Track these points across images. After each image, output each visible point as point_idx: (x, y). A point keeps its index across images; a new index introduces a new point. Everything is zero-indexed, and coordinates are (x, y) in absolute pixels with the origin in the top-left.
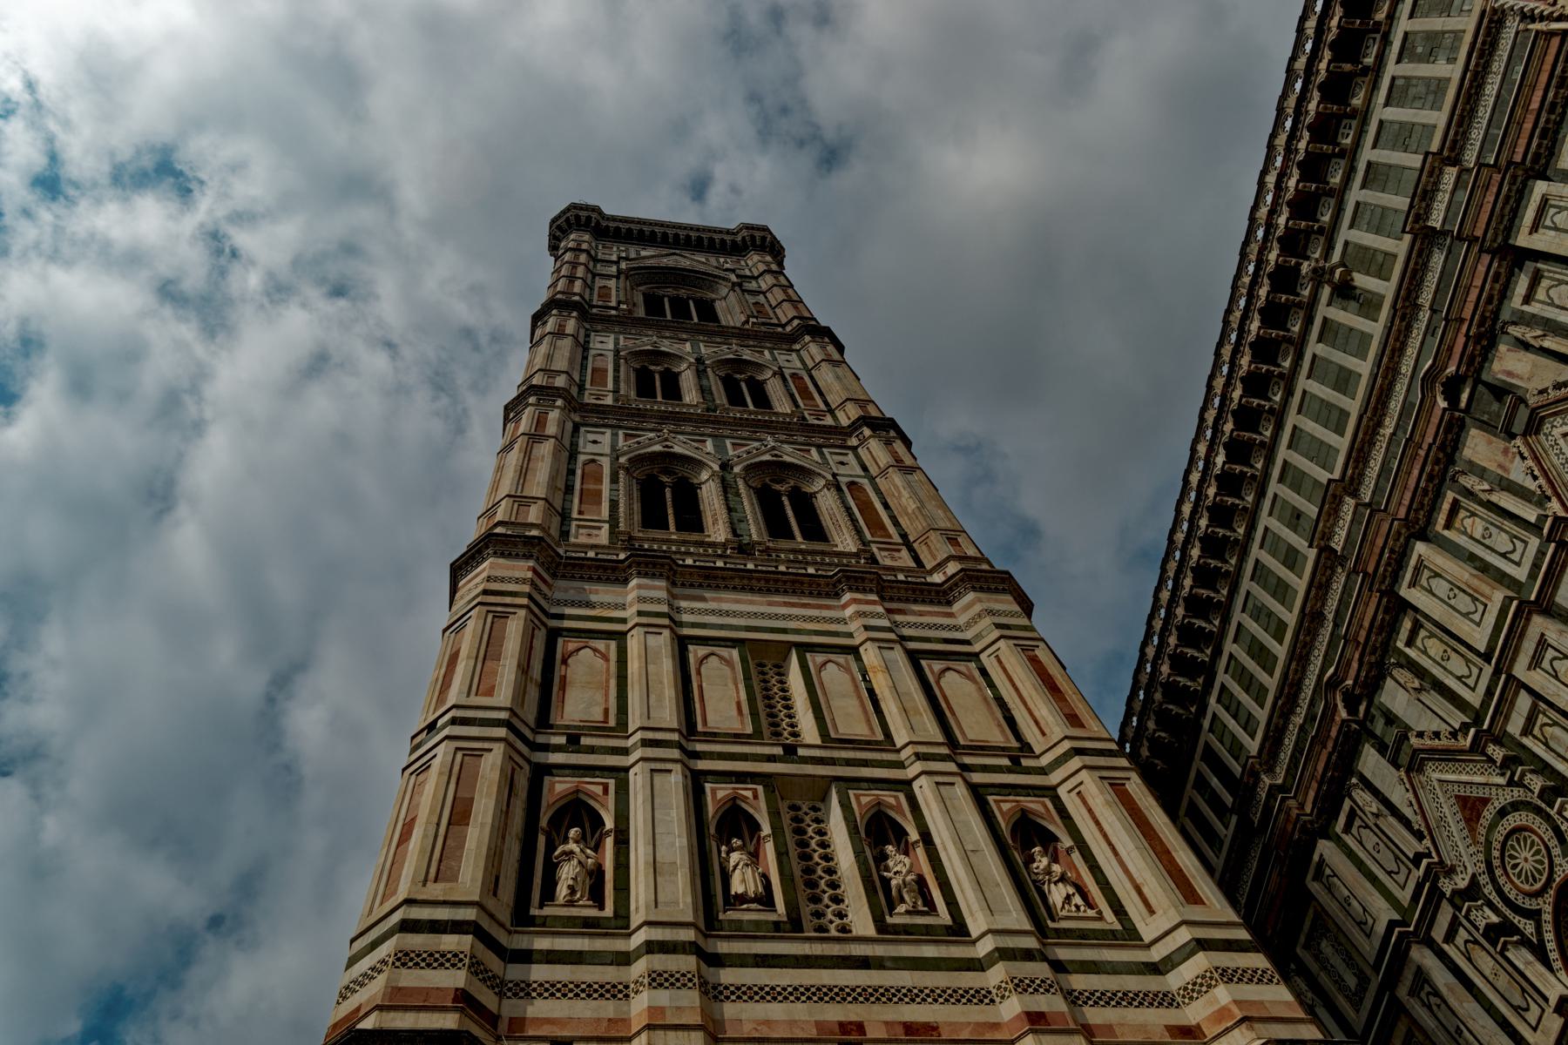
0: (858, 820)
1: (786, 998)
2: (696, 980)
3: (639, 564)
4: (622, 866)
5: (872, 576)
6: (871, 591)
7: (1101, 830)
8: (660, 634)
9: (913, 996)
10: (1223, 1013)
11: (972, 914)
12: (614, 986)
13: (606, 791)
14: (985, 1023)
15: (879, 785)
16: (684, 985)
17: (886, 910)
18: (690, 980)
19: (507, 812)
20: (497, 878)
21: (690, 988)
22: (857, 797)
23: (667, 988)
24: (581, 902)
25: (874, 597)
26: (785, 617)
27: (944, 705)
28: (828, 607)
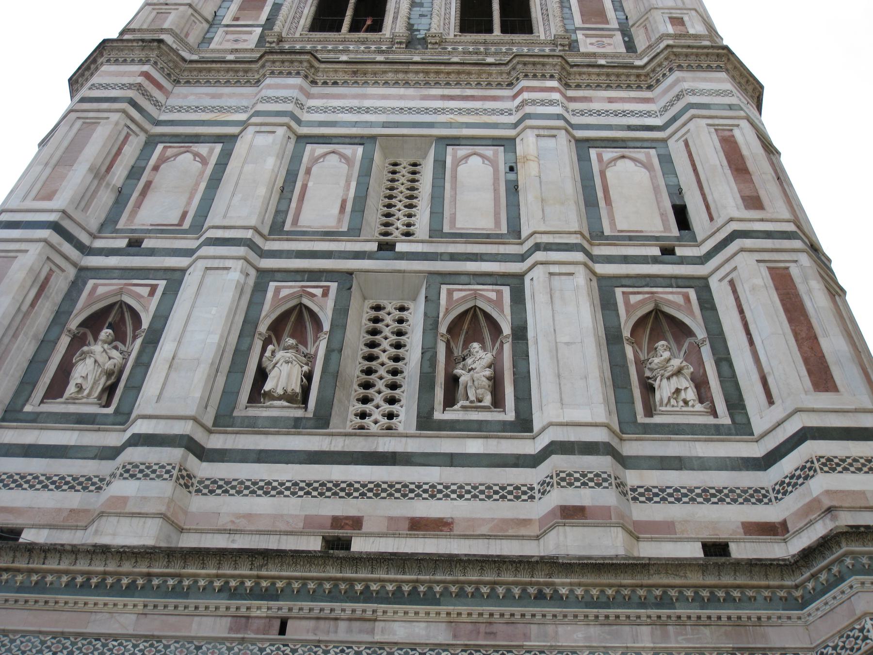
0: (441, 315)
2: (175, 473)
3: (274, 62)
5: (556, 60)
6: (552, 77)
8: (274, 132)
9: (433, 492)
13: (152, 293)
14: (512, 520)
15: (481, 280)
18: (168, 472)
19: (27, 314)
22: (450, 293)
25: (554, 84)
26: (436, 111)
27: (600, 194)
28: (494, 98)
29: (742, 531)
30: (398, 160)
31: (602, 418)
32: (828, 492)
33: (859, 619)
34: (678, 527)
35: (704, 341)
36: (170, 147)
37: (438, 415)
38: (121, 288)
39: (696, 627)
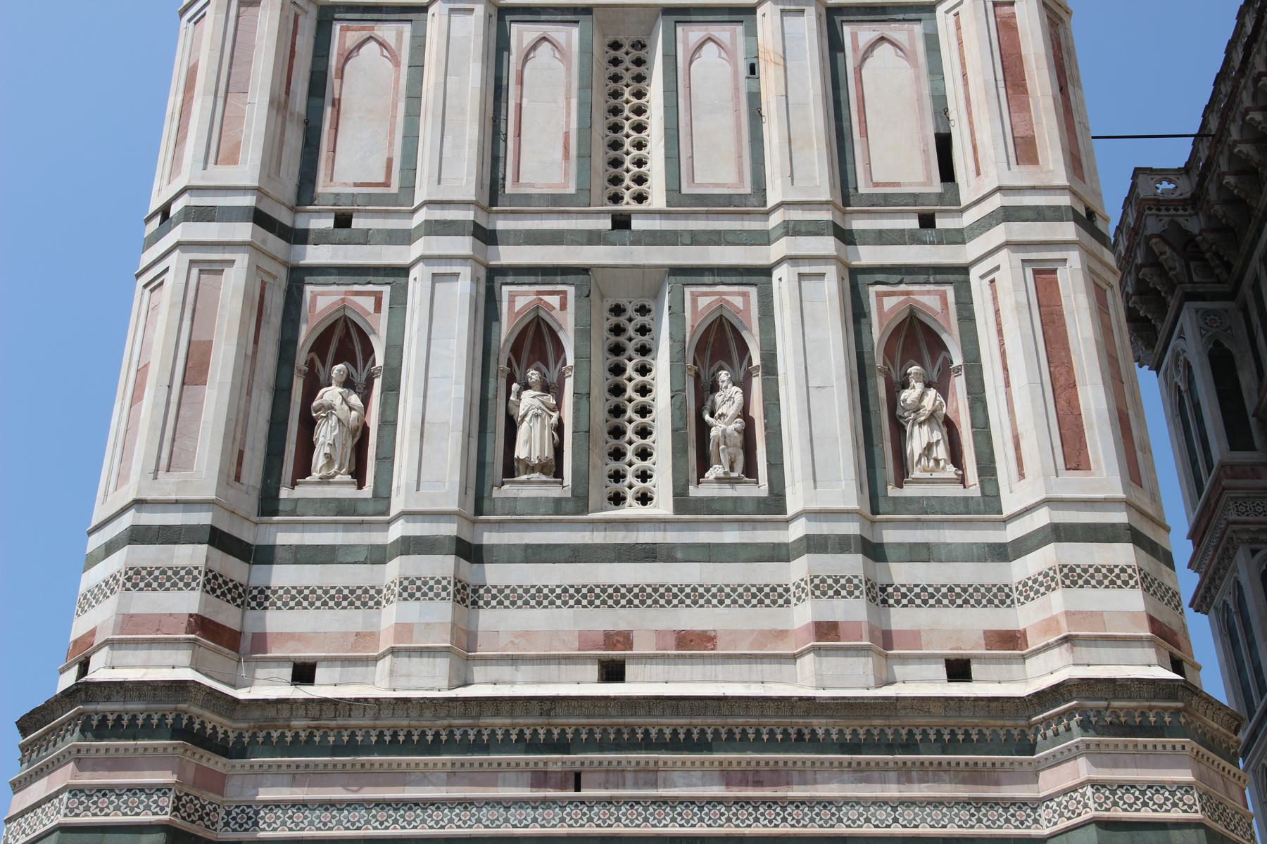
0: (687, 339)
1: (552, 603)
2: (451, 589)
4: (389, 423)
7: (1002, 344)
10: (1051, 623)
11: (793, 484)
12: (366, 592)
13: (378, 308)
14: (770, 631)
16: (437, 595)
17: (693, 476)
18: (445, 589)
20: (241, 454)
21: (443, 599)
22: (695, 298)
23: (418, 599)
24: (338, 478)
29: (983, 642)
30: (620, 38)
31: (854, 505)
32: (1067, 613)
33: (1082, 785)
34: (924, 637)
35: (958, 369)
36: (348, 29)
37: (694, 491)
38: (343, 300)
39: (938, 773)
